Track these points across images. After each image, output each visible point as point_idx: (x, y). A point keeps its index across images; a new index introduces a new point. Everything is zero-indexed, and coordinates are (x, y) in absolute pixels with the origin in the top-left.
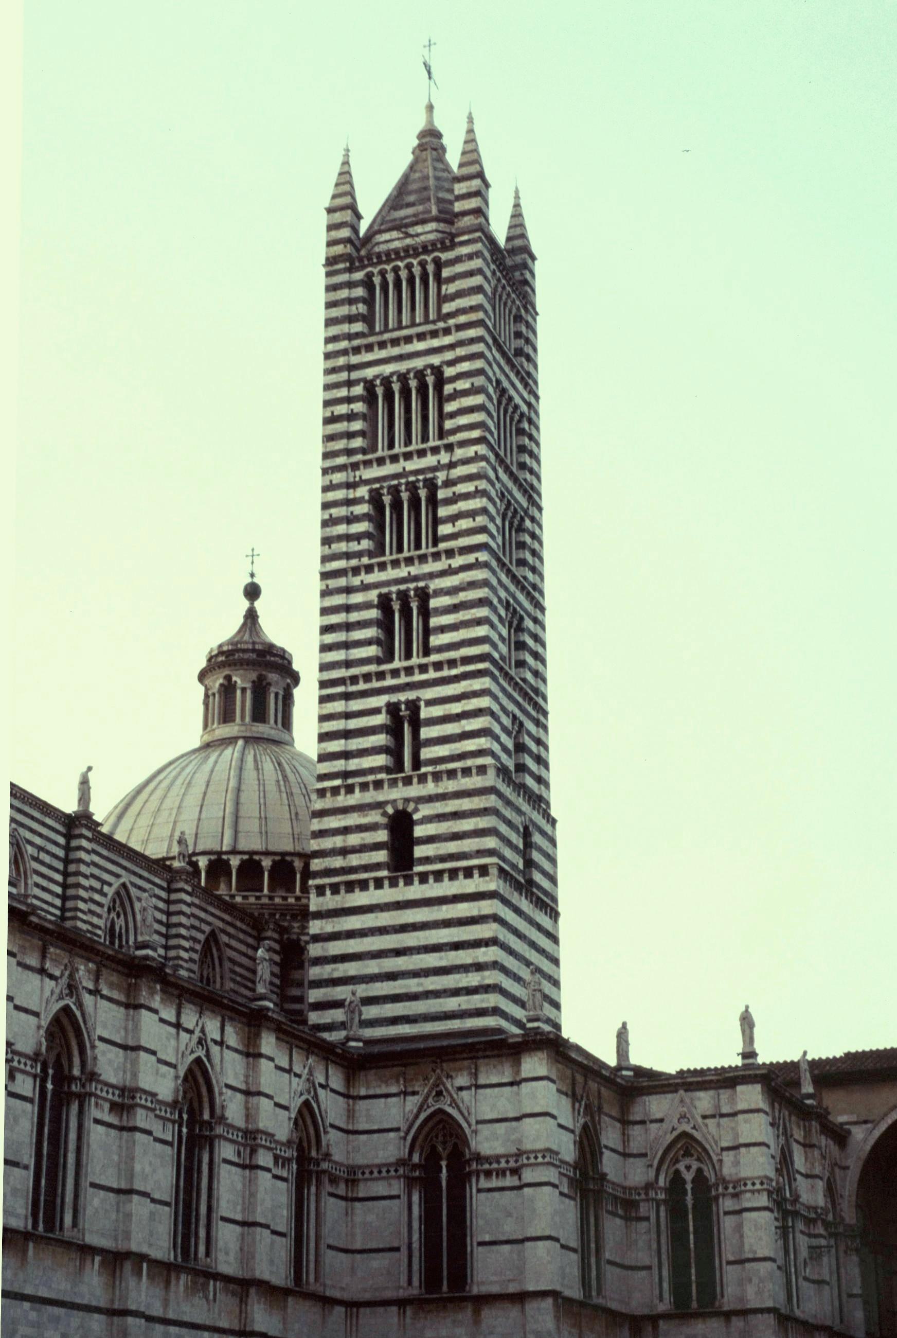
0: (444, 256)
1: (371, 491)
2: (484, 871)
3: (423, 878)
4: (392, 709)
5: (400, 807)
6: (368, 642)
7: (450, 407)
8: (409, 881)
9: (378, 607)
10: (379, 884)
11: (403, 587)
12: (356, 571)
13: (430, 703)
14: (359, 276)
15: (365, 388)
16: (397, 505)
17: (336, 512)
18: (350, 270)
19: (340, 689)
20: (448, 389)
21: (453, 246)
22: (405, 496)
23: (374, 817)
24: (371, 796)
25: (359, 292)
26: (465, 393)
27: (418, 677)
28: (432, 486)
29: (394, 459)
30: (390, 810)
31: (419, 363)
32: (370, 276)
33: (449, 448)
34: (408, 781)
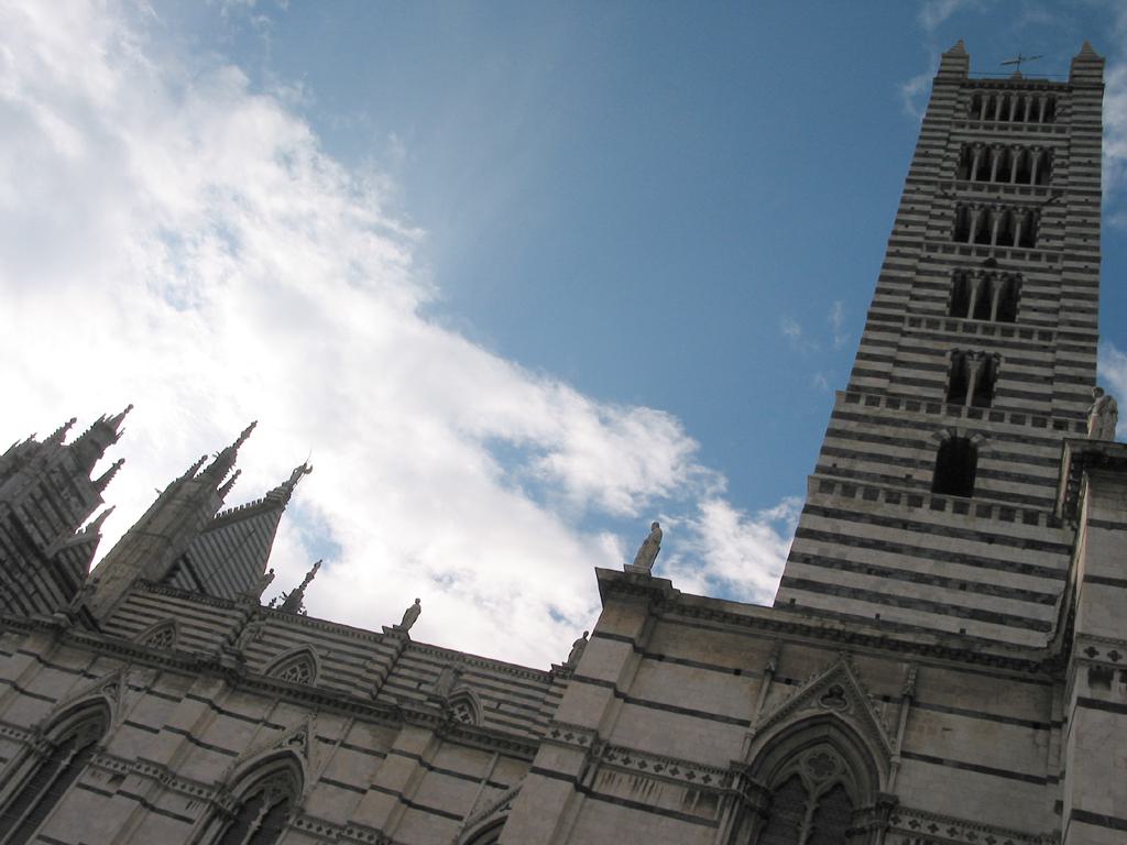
1: (959, 204)
3: (985, 512)
4: (960, 360)
5: (960, 435)
8: (961, 509)
10: (916, 501)
17: (918, 207)
23: (925, 435)
24: (922, 416)
27: (997, 337)
29: (993, 189)
33: (1057, 193)
34: (973, 415)
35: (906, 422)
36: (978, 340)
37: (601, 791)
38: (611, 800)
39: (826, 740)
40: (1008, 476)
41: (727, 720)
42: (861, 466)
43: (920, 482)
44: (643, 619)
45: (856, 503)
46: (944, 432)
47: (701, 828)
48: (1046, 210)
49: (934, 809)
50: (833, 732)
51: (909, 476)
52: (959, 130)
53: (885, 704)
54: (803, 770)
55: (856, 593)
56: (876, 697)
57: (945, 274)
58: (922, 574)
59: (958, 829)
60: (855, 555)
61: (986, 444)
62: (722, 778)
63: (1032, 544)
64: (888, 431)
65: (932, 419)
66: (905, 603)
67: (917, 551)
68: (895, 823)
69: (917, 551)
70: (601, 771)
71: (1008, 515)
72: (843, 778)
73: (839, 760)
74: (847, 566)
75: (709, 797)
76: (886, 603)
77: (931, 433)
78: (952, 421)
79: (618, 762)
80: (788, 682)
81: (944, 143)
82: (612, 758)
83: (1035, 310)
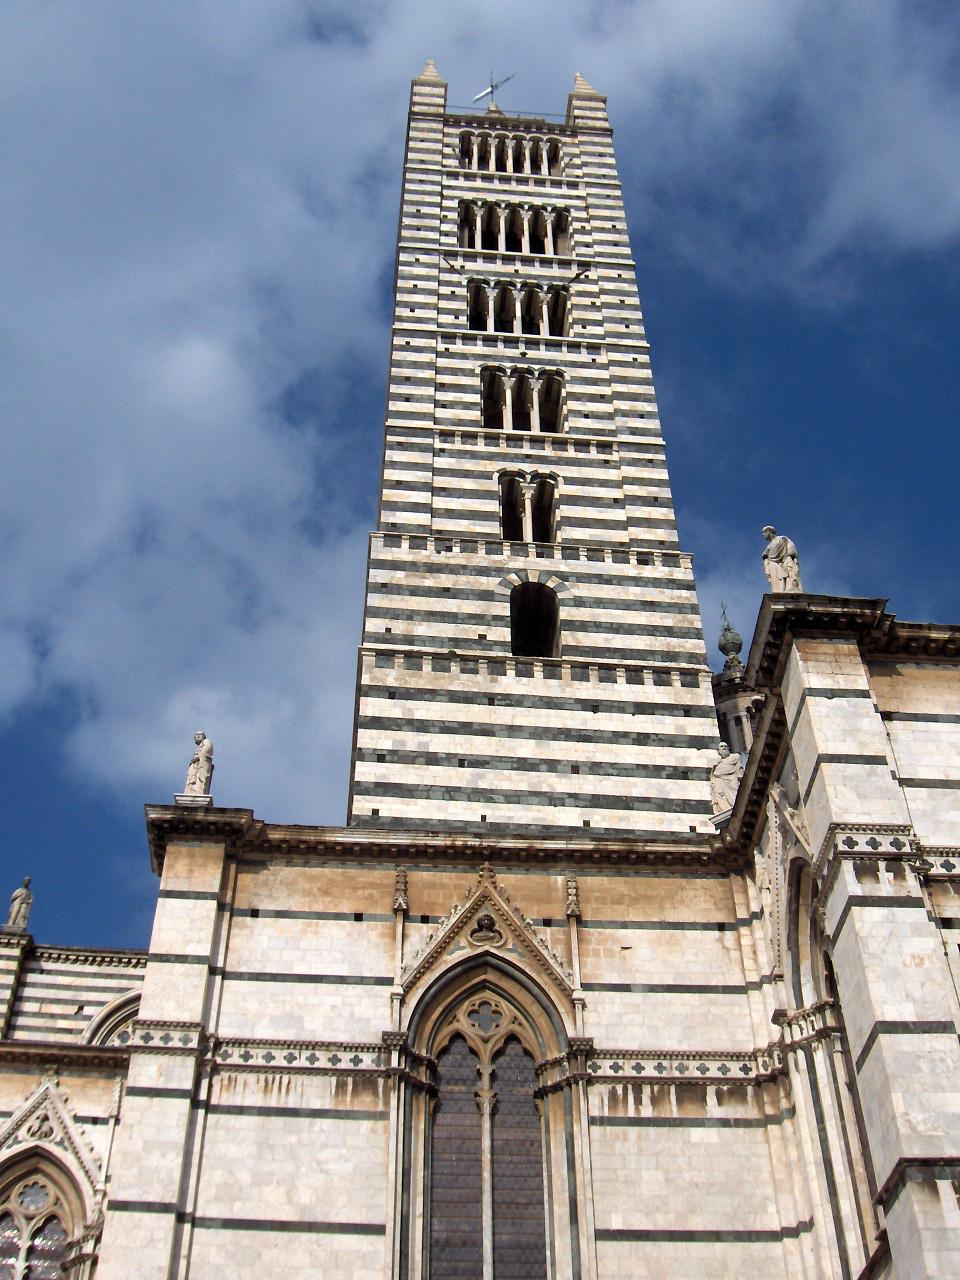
1: (471, 281)
2: (690, 679)
3: (581, 672)
4: (509, 481)
6: (467, 406)
8: (552, 671)
10: (497, 667)
12: (449, 338)
13: (569, 481)
17: (421, 284)
21: (574, 134)
23: (490, 583)
24: (481, 558)
33: (585, 266)
35: (464, 567)
36: (528, 456)
37: (224, 1102)
38: (240, 1110)
39: (484, 986)
40: (598, 627)
41: (361, 981)
42: (422, 629)
43: (496, 643)
44: (221, 865)
46: (513, 577)
47: (366, 1125)
48: (575, 288)
49: (633, 1046)
50: (491, 976)
51: (482, 637)
52: (453, 183)
53: (548, 929)
54: (463, 1023)
55: (451, 793)
56: (536, 922)
57: (470, 373)
58: (525, 759)
59: (665, 1063)
60: (439, 743)
61: (567, 589)
62: (375, 1056)
64: (445, 580)
65: (495, 562)
66: (514, 797)
68: (595, 1071)
69: (513, 731)
70: (216, 1079)
71: (607, 673)
72: (516, 1028)
73: (505, 1006)
74: (432, 759)
75: (364, 1080)
76: (490, 800)
77: (499, 580)
78: (519, 563)
79: (236, 1058)
80: (425, 919)
82: (226, 1055)
83: (586, 416)
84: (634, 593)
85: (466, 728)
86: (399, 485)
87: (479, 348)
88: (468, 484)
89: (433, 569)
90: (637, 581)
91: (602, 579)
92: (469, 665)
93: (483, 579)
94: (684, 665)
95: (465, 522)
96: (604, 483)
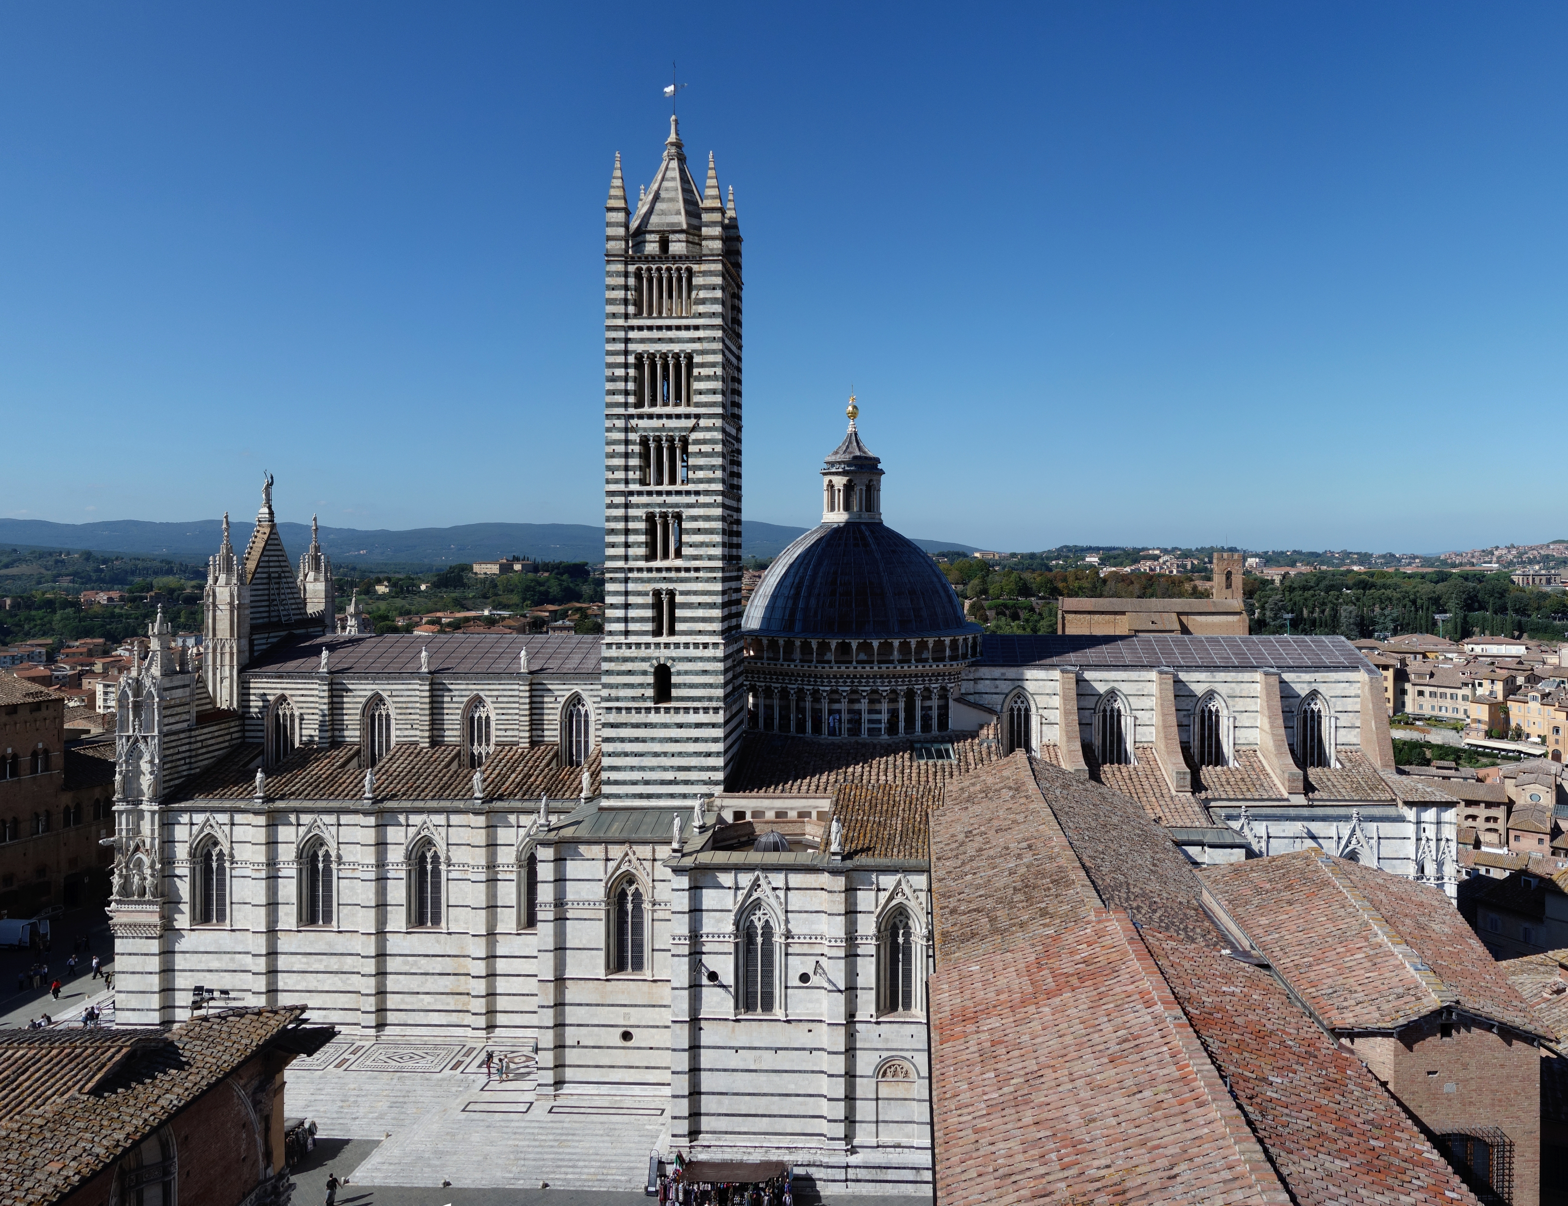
0: (695, 267)
1: (641, 436)
2: (716, 710)
3: (677, 710)
4: (657, 593)
6: (639, 545)
7: (696, 385)
8: (667, 710)
9: (647, 520)
10: (648, 710)
11: (664, 510)
13: (682, 593)
14: (632, 268)
15: (636, 358)
16: (659, 450)
18: (626, 264)
19: (622, 575)
20: (696, 372)
22: (665, 445)
23: (645, 666)
24: (643, 652)
25: (632, 281)
26: (708, 378)
27: (673, 574)
28: (685, 442)
30: (655, 662)
31: (676, 348)
32: (639, 269)
42: (622, 693)
45: (623, 717)
48: (693, 436)
55: (632, 768)
60: (629, 747)
63: (698, 725)
66: (652, 769)
67: (653, 740)
69: (653, 740)
71: (687, 710)
74: (626, 754)
81: (621, 359)
84: (700, 666)
85: (637, 740)
86: (612, 606)
87: (645, 499)
88: (640, 600)
89: (626, 660)
90: (701, 659)
91: (690, 660)
92: (638, 710)
93: (644, 664)
94: (714, 704)
95: (638, 624)
96: (695, 593)
